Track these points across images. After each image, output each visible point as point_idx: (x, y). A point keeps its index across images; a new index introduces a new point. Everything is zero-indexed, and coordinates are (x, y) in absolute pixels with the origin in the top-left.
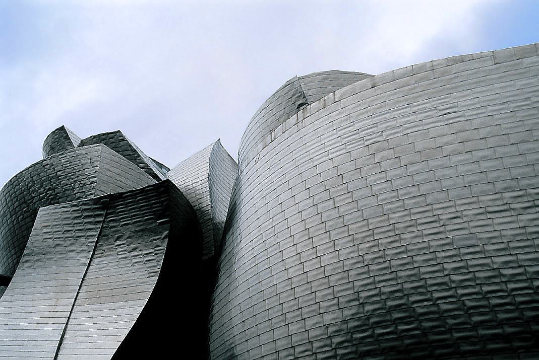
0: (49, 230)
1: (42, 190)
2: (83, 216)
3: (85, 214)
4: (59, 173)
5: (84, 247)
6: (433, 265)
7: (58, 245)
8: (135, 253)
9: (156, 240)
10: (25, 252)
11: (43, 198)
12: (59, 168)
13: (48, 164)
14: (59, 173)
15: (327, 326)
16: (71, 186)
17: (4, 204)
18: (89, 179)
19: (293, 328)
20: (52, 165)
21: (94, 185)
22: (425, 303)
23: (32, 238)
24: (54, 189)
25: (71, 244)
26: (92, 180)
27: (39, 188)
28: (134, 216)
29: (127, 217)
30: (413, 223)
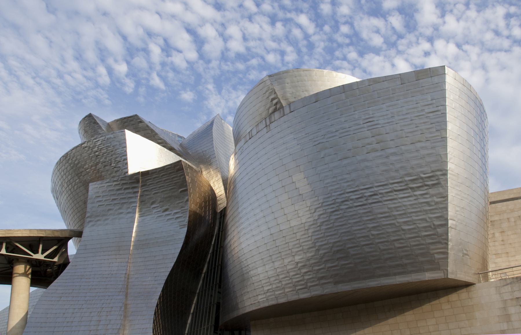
0: (101, 199)
1: (87, 166)
3: (125, 187)
5: (129, 210)
6: (360, 226)
7: (110, 210)
10: (88, 215)
11: (89, 172)
15: (297, 263)
17: (60, 177)
18: (121, 157)
19: (277, 264)
21: (125, 162)
22: (356, 248)
23: (89, 206)
25: (120, 209)
27: (85, 165)
28: (161, 187)
29: (156, 188)
30: (347, 199)
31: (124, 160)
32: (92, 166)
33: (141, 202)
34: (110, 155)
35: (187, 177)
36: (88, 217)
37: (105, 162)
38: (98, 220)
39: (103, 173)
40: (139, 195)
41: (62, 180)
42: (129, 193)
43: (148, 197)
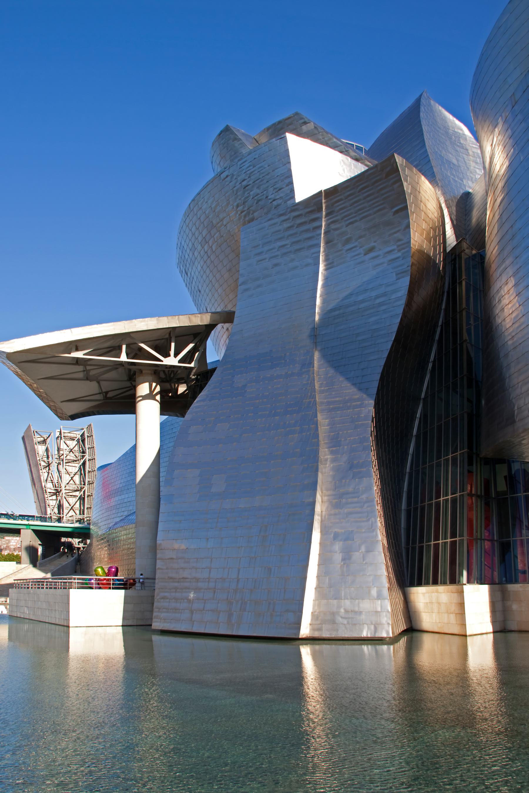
2: (296, 226)
3: (299, 221)
4: (244, 183)
8: (372, 255)
9: (395, 233)
10: (241, 280)
12: (243, 176)
13: (227, 176)
14: (244, 183)
16: (263, 195)
20: (233, 175)
24: (244, 203)
25: (292, 260)
26: (287, 181)
28: (360, 210)
31: (287, 185)
32: (238, 206)
33: (327, 243)
34: (265, 181)
35: (405, 184)
36: (243, 283)
37: (258, 194)
38: (259, 286)
39: (256, 214)
40: (323, 231)
41: (193, 240)
42: (307, 231)
43: (337, 232)
